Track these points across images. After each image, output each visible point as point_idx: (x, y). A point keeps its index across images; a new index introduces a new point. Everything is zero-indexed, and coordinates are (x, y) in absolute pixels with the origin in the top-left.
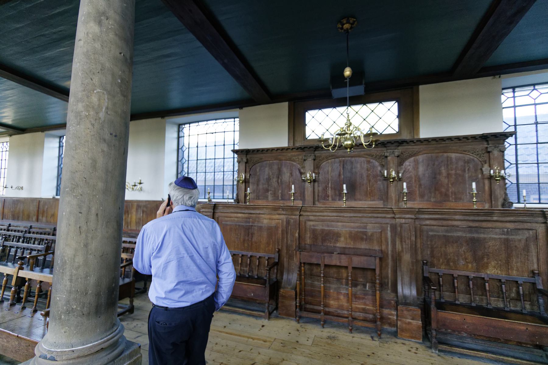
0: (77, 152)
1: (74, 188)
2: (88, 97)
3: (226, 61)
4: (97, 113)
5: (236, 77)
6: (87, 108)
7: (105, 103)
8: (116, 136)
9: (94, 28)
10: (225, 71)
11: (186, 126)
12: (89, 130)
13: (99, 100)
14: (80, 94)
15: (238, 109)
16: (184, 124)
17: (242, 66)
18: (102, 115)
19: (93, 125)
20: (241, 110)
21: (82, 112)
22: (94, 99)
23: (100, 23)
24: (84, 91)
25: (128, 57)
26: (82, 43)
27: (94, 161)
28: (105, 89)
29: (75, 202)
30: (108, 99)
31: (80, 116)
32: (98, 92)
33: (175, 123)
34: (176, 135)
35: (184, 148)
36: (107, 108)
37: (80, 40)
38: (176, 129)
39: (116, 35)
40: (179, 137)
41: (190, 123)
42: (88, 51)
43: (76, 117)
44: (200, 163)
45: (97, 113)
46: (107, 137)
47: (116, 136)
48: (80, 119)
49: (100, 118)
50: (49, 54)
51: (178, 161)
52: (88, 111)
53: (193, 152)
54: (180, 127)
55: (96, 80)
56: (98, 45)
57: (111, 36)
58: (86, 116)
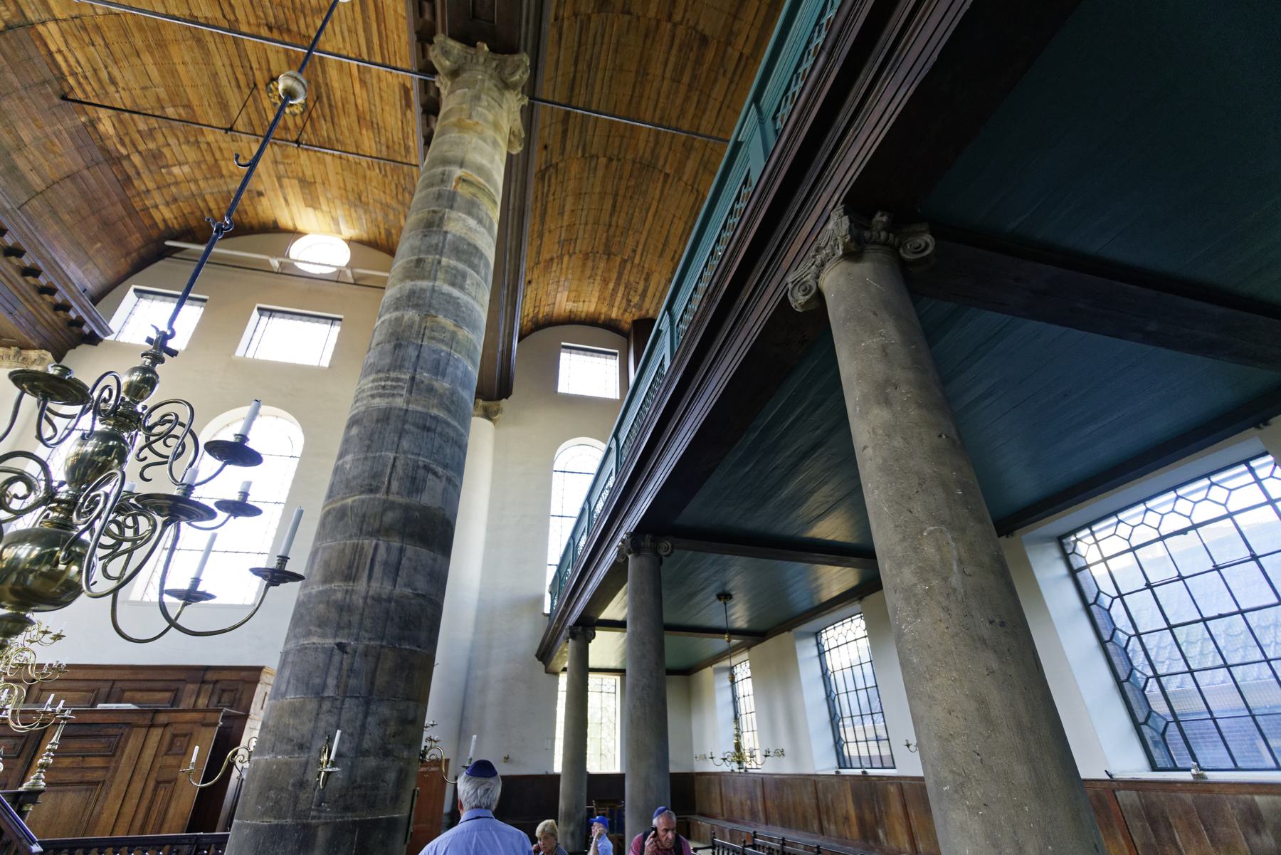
0: (937, 682)
1: (962, 784)
2: (915, 550)
3: (1153, 327)
4: (945, 579)
5: (1207, 348)
6: (922, 573)
7: (953, 551)
8: (1002, 624)
9: (880, 415)
10: (1162, 350)
11: (1079, 535)
12: (943, 626)
13: (939, 549)
14: (898, 548)
15: (1252, 429)
16: (1074, 532)
17: (1218, 310)
18: (955, 580)
19: (946, 610)
20: (1266, 430)
21: (915, 585)
22: (929, 550)
23: (887, 402)
24: (904, 539)
25: (955, 437)
26: (869, 451)
27: (982, 702)
28: (943, 523)
29: (975, 826)
30: (954, 539)
31: (915, 595)
32: (930, 533)
33: (1048, 539)
34: (1062, 569)
35: (1106, 601)
36: (960, 562)
37: (865, 448)
38: (1055, 552)
39: (919, 406)
40: (1073, 573)
41: (1089, 525)
42: (885, 460)
43: (906, 599)
44: (1245, 647)
45: (945, 579)
46: (985, 630)
47: (1002, 624)
48: (918, 603)
49: (955, 590)
50: (785, 493)
51: (1102, 643)
52: (926, 581)
53: (1142, 605)
54: (1061, 542)
55: (918, 508)
56: (898, 442)
57: (914, 412)
58: (927, 592)
